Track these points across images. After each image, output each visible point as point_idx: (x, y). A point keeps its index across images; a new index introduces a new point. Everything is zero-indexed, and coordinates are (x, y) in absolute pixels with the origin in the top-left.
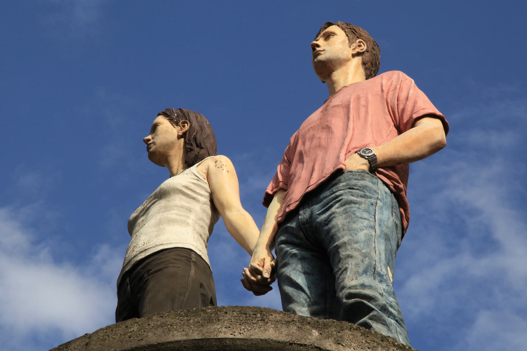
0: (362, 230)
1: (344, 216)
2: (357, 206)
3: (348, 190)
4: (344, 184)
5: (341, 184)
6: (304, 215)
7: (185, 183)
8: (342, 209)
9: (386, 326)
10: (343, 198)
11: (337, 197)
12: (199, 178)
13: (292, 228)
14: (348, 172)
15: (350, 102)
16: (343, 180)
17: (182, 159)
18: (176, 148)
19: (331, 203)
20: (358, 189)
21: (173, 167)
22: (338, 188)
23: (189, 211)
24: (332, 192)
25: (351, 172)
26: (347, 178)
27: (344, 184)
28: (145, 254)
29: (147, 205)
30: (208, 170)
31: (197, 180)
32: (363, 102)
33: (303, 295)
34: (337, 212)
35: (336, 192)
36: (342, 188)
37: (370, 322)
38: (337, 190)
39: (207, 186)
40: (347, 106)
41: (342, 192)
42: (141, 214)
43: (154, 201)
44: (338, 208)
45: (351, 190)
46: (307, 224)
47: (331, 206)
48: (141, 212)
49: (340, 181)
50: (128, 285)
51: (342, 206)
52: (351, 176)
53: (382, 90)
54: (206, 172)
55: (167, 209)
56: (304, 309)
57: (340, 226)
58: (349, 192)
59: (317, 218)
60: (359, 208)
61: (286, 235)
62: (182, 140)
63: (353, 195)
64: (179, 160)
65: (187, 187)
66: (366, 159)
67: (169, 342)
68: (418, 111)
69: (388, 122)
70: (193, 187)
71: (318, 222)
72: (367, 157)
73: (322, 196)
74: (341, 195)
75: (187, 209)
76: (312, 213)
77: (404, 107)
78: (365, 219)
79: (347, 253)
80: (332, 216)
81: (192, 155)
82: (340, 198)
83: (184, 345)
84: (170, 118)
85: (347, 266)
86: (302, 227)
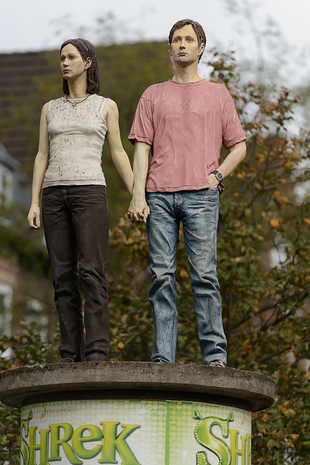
0: (212, 231)
1: (205, 219)
2: (211, 213)
3: (208, 201)
4: (207, 197)
5: (206, 197)
6: (179, 200)
7: (100, 128)
11: (202, 204)
12: (104, 122)
20: (212, 201)
23: (99, 148)
24: (200, 199)
25: (212, 190)
26: (209, 194)
27: (207, 197)
28: (81, 183)
30: (108, 114)
33: (168, 248)
37: (212, 295)
38: (203, 199)
39: (106, 128)
41: (205, 202)
42: (67, 133)
45: (210, 202)
47: (198, 208)
48: (66, 132)
49: (205, 194)
51: (204, 211)
52: (211, 193)
56: (168, 257)
58: (209, 203)
60: (212, 215)
62: (86, 72)
63: (210, 206)
65: (99, 131)
69: (220, 136)
72: (219, 181)
74: (205, 204)
79: (206, 248)
80: (197, 216)
85: (205, 257)
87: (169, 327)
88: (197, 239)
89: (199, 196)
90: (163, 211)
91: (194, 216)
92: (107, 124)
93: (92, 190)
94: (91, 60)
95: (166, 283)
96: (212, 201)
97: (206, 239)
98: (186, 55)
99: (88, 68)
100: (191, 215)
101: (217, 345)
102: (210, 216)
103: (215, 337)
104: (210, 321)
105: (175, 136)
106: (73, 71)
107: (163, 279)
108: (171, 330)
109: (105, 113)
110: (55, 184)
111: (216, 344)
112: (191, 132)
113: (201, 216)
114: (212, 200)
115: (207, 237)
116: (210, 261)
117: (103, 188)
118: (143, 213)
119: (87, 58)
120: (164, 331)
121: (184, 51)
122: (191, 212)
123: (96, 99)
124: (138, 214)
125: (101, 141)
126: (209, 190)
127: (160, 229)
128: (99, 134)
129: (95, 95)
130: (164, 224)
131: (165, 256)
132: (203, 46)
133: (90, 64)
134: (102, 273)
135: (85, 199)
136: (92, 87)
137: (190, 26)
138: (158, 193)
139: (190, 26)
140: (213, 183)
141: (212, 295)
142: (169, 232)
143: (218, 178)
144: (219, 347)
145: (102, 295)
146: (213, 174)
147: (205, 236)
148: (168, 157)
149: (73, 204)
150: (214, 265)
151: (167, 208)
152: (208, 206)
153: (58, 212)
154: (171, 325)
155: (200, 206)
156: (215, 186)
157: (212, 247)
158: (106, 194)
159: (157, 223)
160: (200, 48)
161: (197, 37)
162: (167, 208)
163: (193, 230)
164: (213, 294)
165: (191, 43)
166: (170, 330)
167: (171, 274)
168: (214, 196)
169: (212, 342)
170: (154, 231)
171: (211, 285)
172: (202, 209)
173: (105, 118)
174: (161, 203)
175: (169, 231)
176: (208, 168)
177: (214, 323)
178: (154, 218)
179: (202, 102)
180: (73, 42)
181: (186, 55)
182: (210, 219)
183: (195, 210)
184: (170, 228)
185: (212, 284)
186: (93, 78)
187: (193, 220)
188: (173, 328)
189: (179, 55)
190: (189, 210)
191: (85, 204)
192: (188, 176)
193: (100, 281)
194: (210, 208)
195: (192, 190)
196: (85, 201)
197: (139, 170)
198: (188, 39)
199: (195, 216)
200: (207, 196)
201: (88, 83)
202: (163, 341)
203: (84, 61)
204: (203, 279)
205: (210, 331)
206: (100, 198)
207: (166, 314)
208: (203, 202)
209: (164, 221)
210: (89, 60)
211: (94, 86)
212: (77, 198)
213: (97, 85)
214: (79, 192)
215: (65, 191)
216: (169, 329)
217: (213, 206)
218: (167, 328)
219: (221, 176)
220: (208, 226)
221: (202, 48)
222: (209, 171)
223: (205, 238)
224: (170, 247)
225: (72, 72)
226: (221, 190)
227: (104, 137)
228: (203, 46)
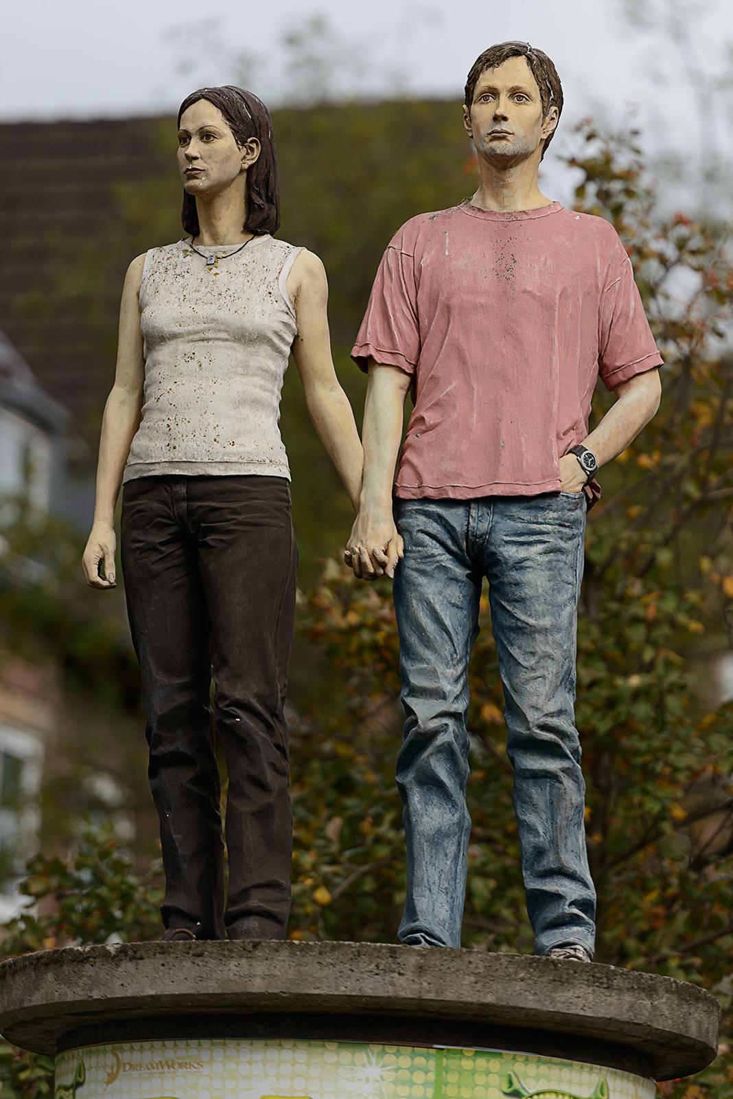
1: (548, 573)
2: (564, 558)
3: (557, 527)
4: (555, 515)
5: (552, 515)
6: (481, 521)
7: (278, 327)
8: (546, 558)
9: (577, 785)
11: (541, 533)
12: (289, 309)
14: (563, 496)
19: (532, 538)
20: (568, 527)
22: (545, 519)
24: (535, 521)
25: (568, 497)
26: (560, 507)
27: (555, 515)
28: (226, 470)
30: (299, 289)
33: (448, 647)
35: (542, 523)
37: (561, 774)
38: (543, 521)
39: (294, 326)
42: (191, 337)
45: (562, 529)
47: (530, 544)
48: (189, 333)
49: (549, 508)
51: (546, 552)
52: (565, 505)
56: (448, 671)
58: (559, 532)
60: (566, 563)
62: (245, 175)
63: (561, 538)
65: (276, 333)
69: (594, 354)
72: (588, 473)
78: (570, 583)
79: (549, 650)
80: (528, 563)
82: (545, 538)
85: (546, 673)
87: (446, 855)
88: (524, 625)
89: (533, 512)
90: (437, 550)
91: (519, 565)
92: (296, 314)
93: (254, 489)
94: (257, 144)
95: (441, 739)
96: (568, 527)
97: (548, 627)
98: (509, 137)
100: (511, 563)
101: (571, 904)
102: (562, 564)
103: (566, 882)
104: (554, 842)
105: (474, 351)
107: (435, 728)
108: (452, 862)
109: (293, 286)
110: (158, 471)
111: (567, 903)
113: (538, 565)
114: (567, 524)
115: (553, 620)
116: (559, 684)
117: (283, 485)
118: (386, 553)
119: (249, 140)
120: (434, 865)
121: (504, 126)
122: (511, 553)
123: (268, 248)
124: (373, 556)
125: (280, 359)
126: (561, 497)
127: (430, 597)
128: (276, 341)
129: (267, 238)
130: (440, 585)
131: (441, 669)
132: (554, 116)
133: (255, 154)
134: (275, 709)
135: (234, 511)
136: (259, 217)
137: (521, 62)
138: (427, 500)
139: (522, 60)
140: (571, 478)
141: (561, 774)
142: (454, 605)
143: (584, 465)
144: (575, 911)
145: (273, 766)
146: (572, 457)
147: (547, 619)
148: (454, 406)
149: (202, 525)
150: (567, 695)
151: (449, 543)
152: (557, 540)
153: (162, 544)
154: (452, 849)
155: (535, 538)
156: (577, 485)
157: (565, 647)
158: (289, 502)
159: (421, 580)
160: (547, 119)
161: (541, 89)
162: (449, 543)
163: (516, 601)
164: (564, 770)
165: (524, 106)
166: (448, 862)
167: (454, 715)
168: (573, 514)
169: (558, 897)
170: (414, 601)
171: (559, 746)
172: (540, 547)
173: (293, 299)
174: (434, 528)
175: (453, 601)
176: (558, 438)
177: (565, 845)
178: (414, 567)
179: (548, 264)
180: (215, 97)
181: (509, 137)
182: (560, 575)
183: (521, 547)
184: (456, 593)
185: (563, 745)
186: (262, 192)
187: (516, 575)
188: (456, 857)
189: (490, 137)
190: (506, 548)
191: (234, 524)
192: (506, 459)
193: (269, 728)
194: (562, 544)
195: (517, 494)
196: (234, 517)
197: (377, 438)
198: (517, 94)
199: (523, 564)
200: (554, 512)
201: (250, 205)
202: (430, 890)
203: (241, 147)
204: (538, 731)
205: (553, 866)
206: (275, 511)
207: (440, 820)
209: (441, 576)
210: (254, 146)
211: (265, 215)
212: (215, 509)
213: (274, 212)
214: (220, 493)
215: (182, 490)
216: (447, 860)
217: (570, 539)
218: (441, 856)
219: (593, 462)
220: (556, 592)
221: (553, 119)
222: (563, 448)
223: (546, 622)
224: (453, 645)
225: (207, 175)
226: (591, 496)
227: (287, 350)
228: (554, 116)
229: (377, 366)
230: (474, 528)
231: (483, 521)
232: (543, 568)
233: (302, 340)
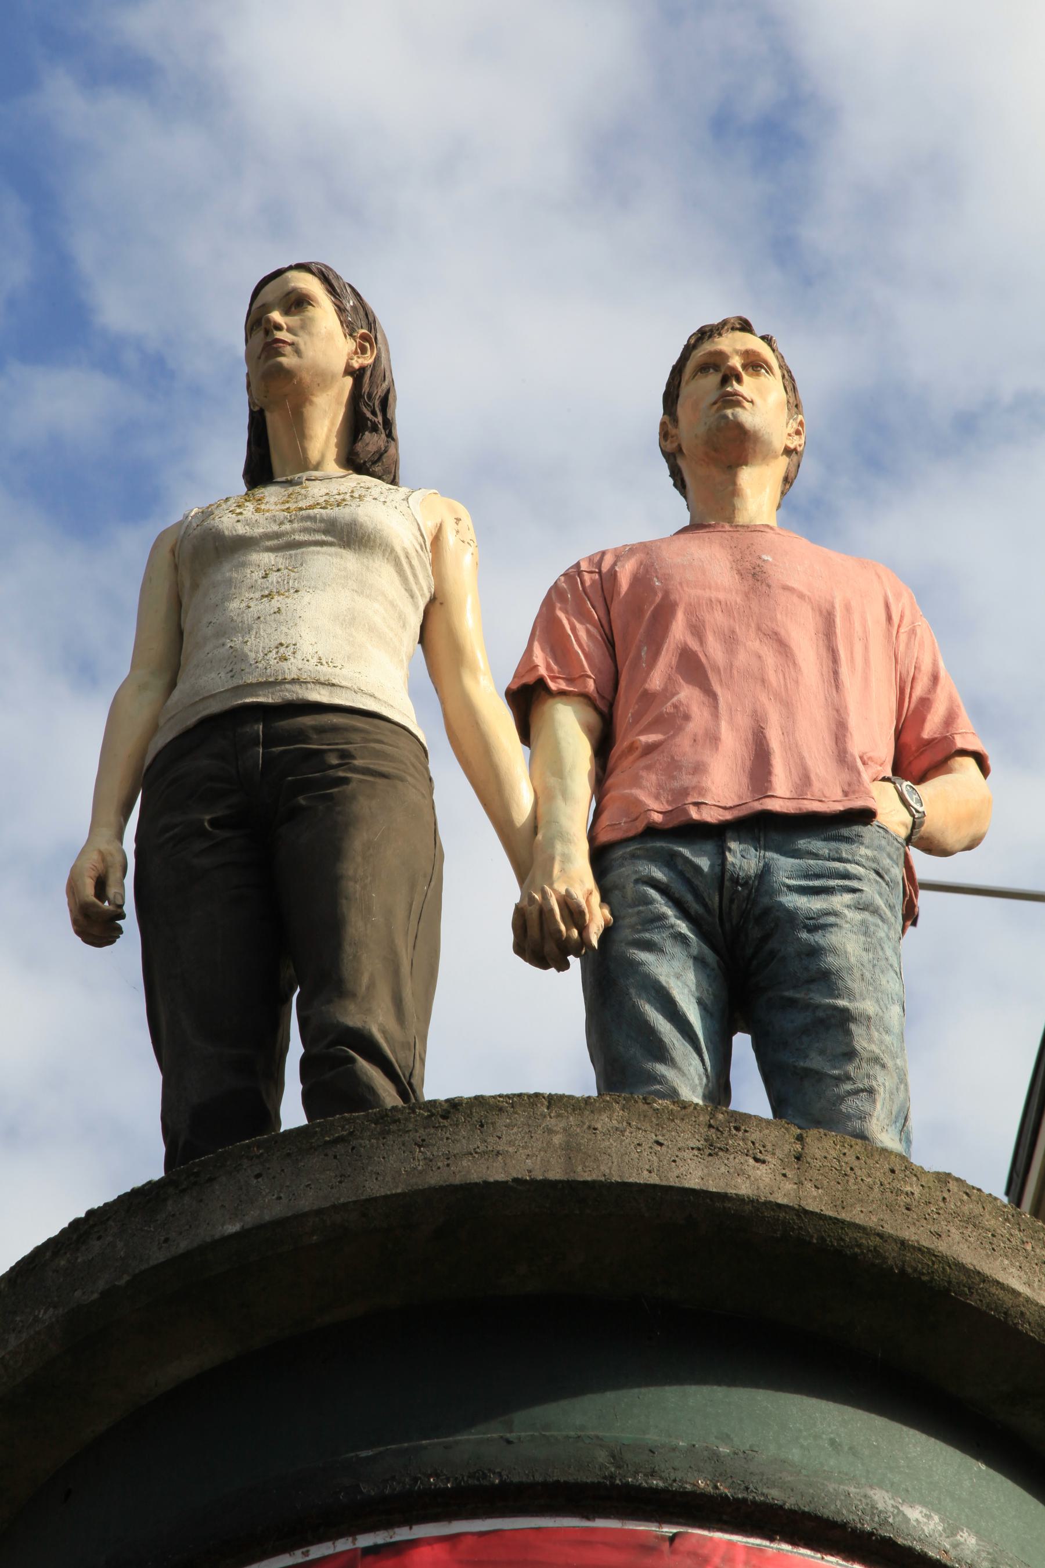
1: (862, 938)
3: (874, 876)
4: (869, 853)
5: (863, 851)
7: (408, 545)
10: (864, 889)
11: (847, 876)
12: (425, 542)
13: (697, 869)
15: (833, 607)
16: (866, 841)
17: (338, 432)
18: (332, 393)
19: (832, 883)
21: (311, 437)
24: (836, 856)
25: (886, 831)
26: (876, 842)
27: (869, 853)
29: (294, 532)
31: (421, 546)
32: (857, 626)
34: (846, 916)
36: (863, 861)
38: (850, 857)
40: (825, 612)
43: (324, 538)
44: (848, 907)
46: (742, 886)
50: (258, 745)
52: (884, 842)
53: (889, 618)
54: (434, 534)
55: (363, 588)
57: (853, 960)
58: (877, 882)
59: (780, 892)
61: (666, 870)
62: (349, 381)
64: (330, 430)
66: (913, 816)
67: (998, 1283)
68: (966, 733)
70: (415, 562)
71: (781, 904)
73: (803, 844)
75: (400, 617)
76: (765, 872)
77: (928, 696)
80: (832, 919)
81: (372, 442)
82: (854, 884)
83: (1023, 1309)
84: (338, 303)
86: (727, 884)
88: (829, 1012)
89: (834, 845)
91: (817, 924)
99: (363, 369)
106: (302, 347)
112: (783, 647)
113: (847, 922)
138: (651, 832)
151: (689, 898)
155: (841, 882)
159: (644, 956)
162: (689, 898)
163: (811, 981)
172: (848, 898)
178: (630, 938)
190: (789, 898)
191: (344, 771)
200: (867, 847)
208: (852, 868)
229: (550, 702)
230: (733, 865)
231: (749, 856)
232: (855, 929)
233: (441, 604)
